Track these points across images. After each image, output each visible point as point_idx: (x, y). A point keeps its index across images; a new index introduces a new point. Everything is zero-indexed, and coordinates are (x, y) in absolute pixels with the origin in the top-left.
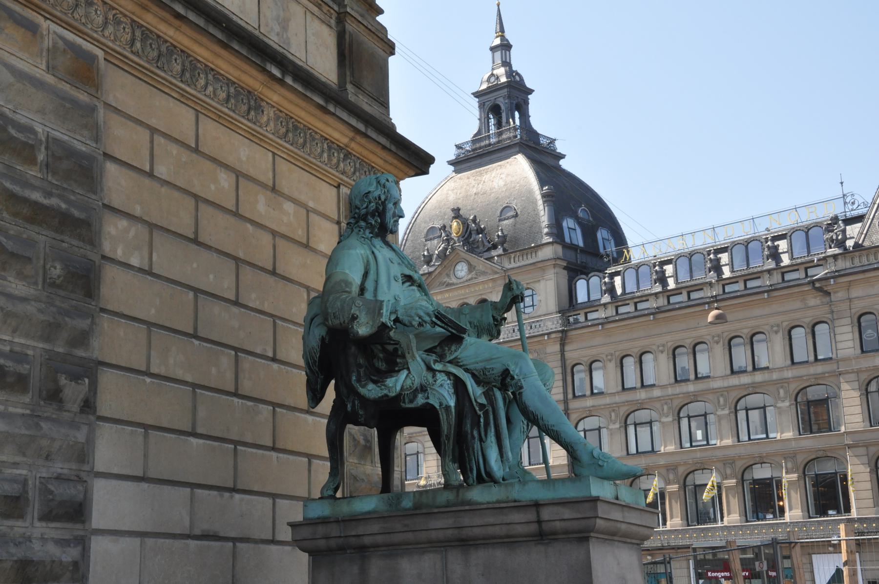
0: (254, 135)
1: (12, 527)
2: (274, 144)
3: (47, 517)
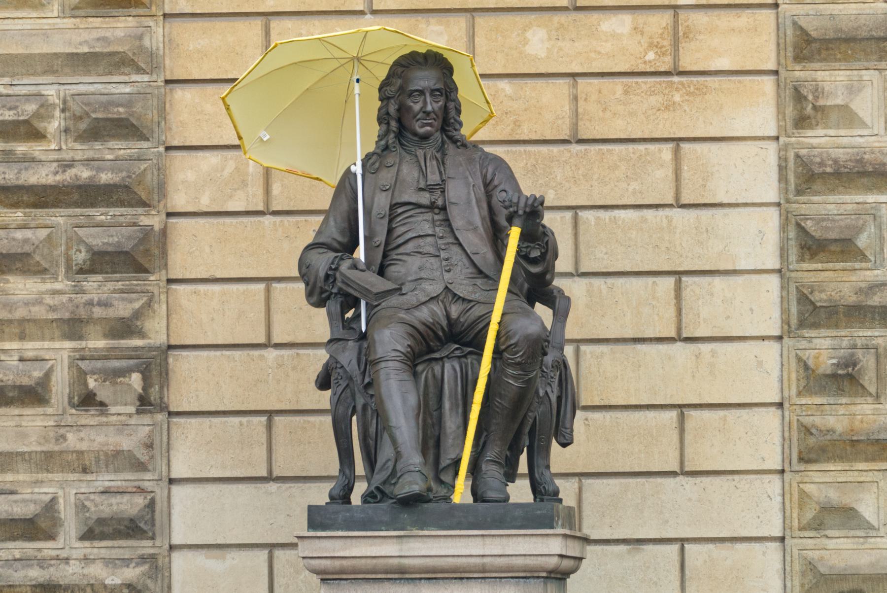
1: (39, 550)
3: (89, 535)
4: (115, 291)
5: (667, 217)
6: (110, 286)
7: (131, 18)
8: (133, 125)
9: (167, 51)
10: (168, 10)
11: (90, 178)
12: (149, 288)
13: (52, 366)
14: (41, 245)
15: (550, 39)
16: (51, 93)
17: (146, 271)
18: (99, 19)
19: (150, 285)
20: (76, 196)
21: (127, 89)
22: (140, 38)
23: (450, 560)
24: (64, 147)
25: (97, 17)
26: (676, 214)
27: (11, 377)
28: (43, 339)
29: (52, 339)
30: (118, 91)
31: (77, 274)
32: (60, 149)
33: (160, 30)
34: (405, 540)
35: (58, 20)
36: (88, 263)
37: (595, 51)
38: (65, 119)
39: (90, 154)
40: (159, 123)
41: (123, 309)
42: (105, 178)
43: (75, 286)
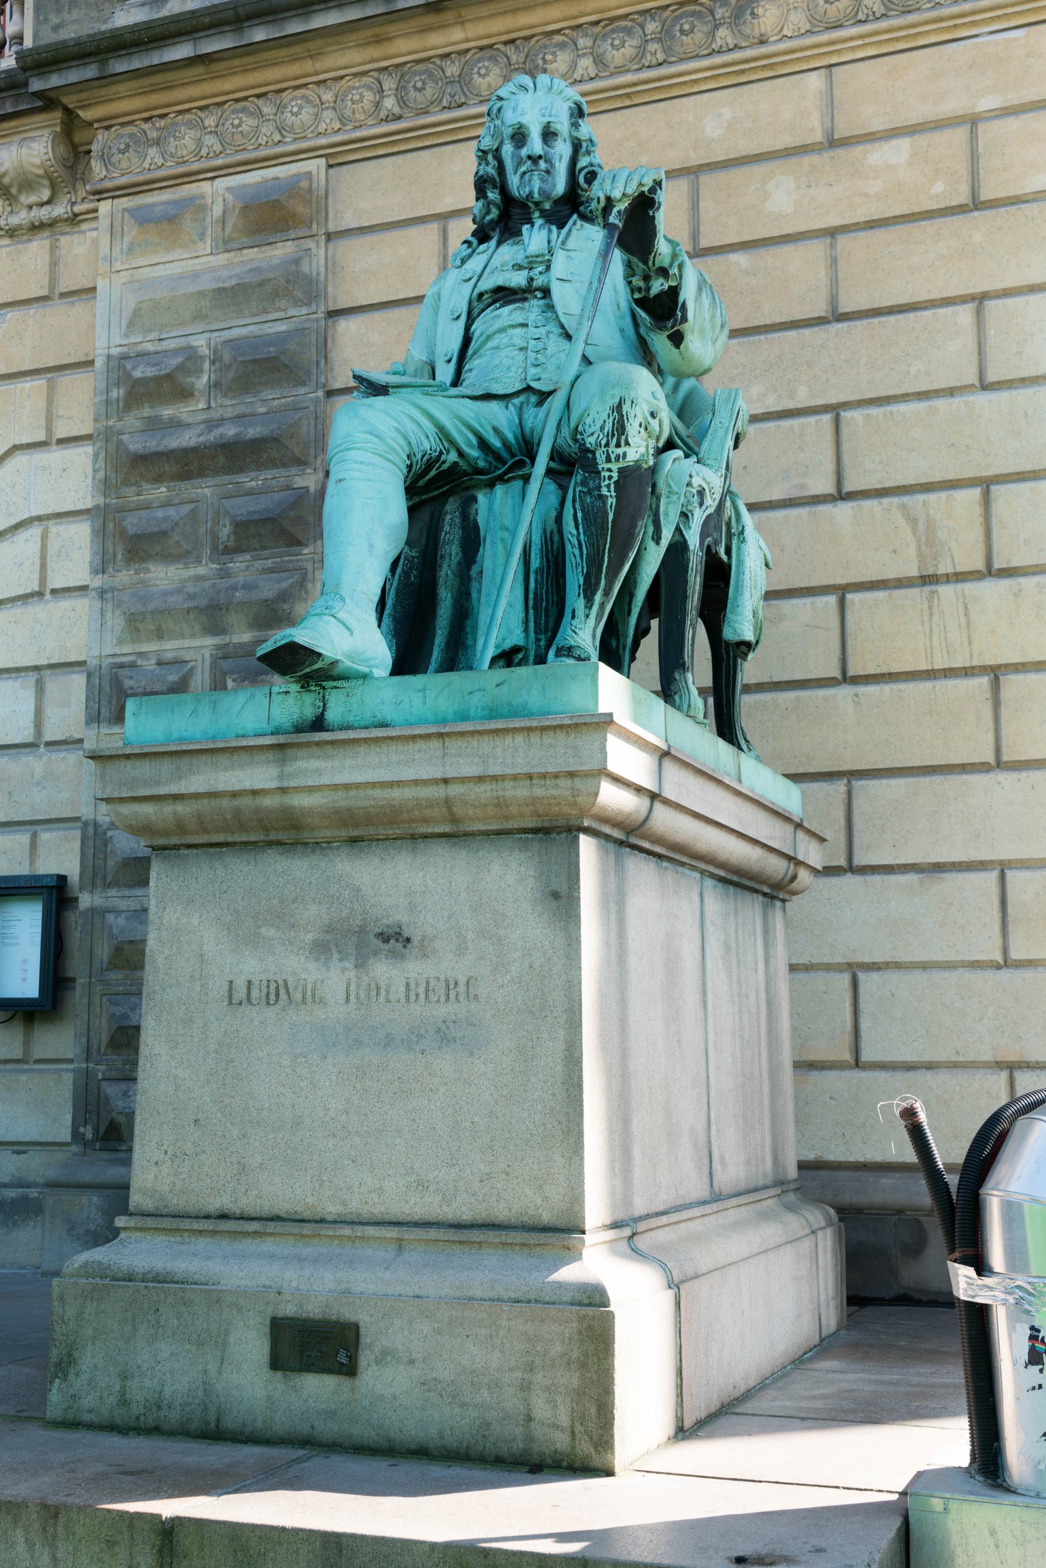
0: (743, 72)
2: (809, 53)
4: (264, 571)
5: (967, 403)
6: (259, 564)
7: (290, 242)
8: (285, 365)
9: (330, 277)
10: (332, 227)
11: (236, 435)
12: (301, 564)
13: (192, 669)
14: (181, 523)
15: (798, 188)
16: (200, 342)
17: (299, 543)
18: (256, 249)
19: (303, 560)
20: (221, 460)
21: (282, 327)
22: (297, 262)
23: (378, 793)
24: (213, 405)
25: (253, 247)
26: (982, 400)
27: (144, 683)
28: (182, 636)
29: (193, 636)
30: (272, 331)
31: (223, 554)
32: (209, 408)
33: (322, 252)
34: (290, 752)
35: (211, 258)
36: (232, 538)
37: (860, 194)
38: (215, 372)
39: (241, 409)
40: (318, 363)
41: (268, 589)
42: (252, 433)
43: (220, 569)
